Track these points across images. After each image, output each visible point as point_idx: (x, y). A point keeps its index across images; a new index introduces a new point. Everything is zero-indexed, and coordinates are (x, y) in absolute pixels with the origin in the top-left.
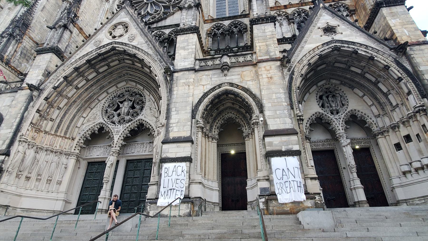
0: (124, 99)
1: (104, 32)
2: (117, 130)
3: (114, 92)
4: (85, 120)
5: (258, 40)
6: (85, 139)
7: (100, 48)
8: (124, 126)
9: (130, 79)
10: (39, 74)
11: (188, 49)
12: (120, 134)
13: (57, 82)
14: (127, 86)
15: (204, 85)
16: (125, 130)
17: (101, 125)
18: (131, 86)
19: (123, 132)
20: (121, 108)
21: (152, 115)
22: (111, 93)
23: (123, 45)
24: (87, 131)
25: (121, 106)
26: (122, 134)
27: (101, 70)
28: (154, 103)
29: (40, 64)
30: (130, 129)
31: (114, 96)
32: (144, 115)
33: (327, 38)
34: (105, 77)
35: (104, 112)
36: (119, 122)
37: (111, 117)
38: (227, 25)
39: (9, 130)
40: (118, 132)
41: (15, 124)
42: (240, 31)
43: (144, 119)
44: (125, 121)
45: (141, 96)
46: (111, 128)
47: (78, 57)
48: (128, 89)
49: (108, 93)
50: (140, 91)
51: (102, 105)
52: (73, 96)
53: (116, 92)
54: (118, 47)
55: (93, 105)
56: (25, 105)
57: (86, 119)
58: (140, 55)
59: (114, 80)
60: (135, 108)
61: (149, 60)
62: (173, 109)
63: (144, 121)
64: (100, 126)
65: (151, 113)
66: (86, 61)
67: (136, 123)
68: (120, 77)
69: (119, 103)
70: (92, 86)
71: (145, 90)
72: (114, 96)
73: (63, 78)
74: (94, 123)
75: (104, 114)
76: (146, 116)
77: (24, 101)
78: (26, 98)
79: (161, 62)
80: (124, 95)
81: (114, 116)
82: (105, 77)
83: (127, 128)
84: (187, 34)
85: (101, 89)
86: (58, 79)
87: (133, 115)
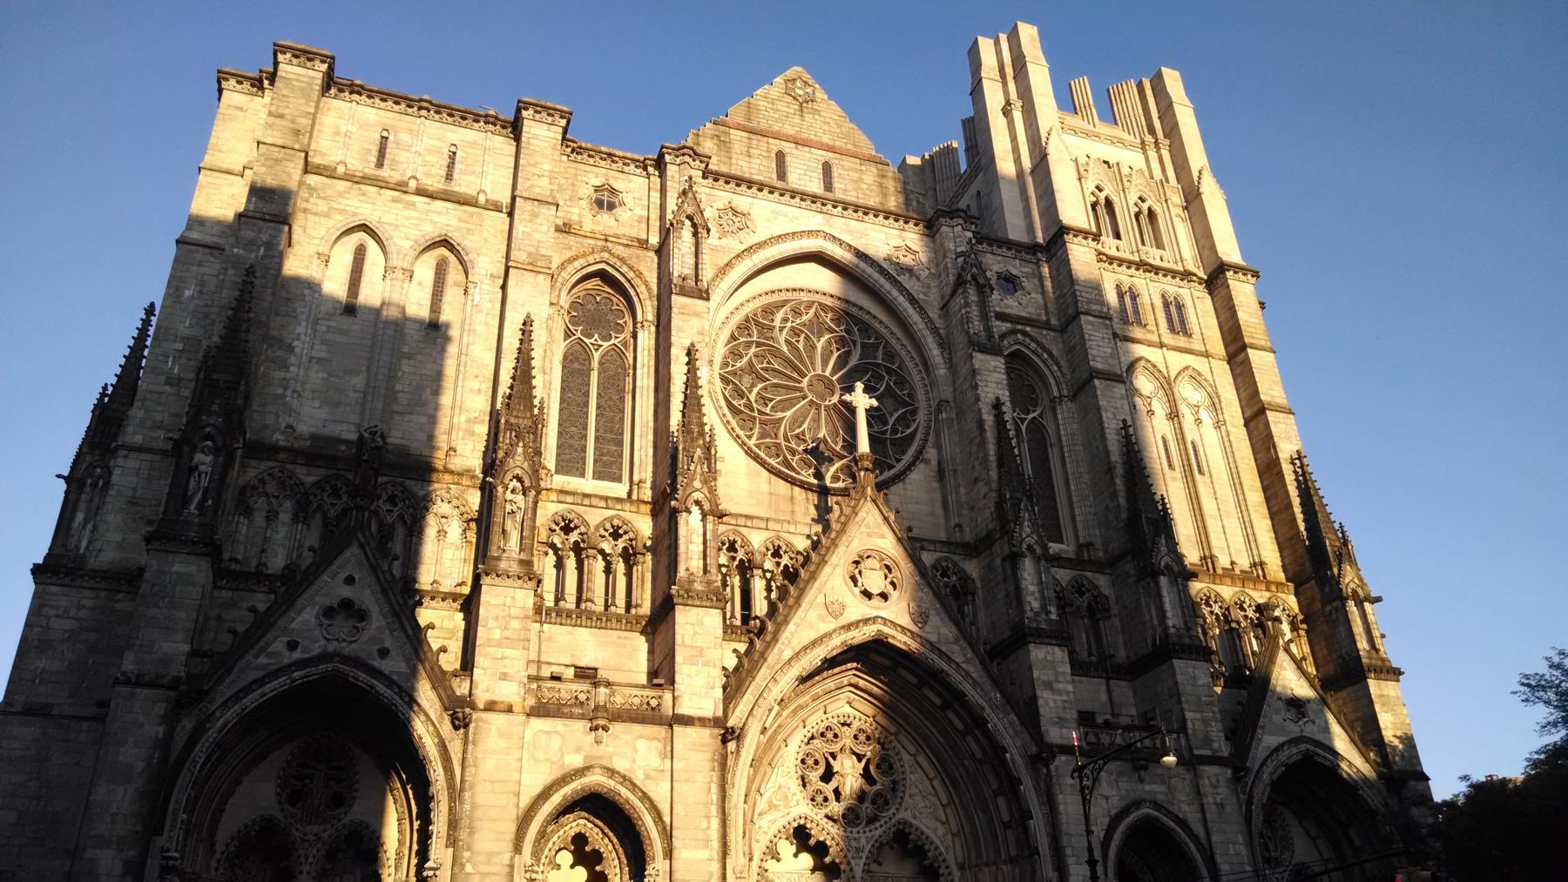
1: (839, 571)
5: (1187, 702)
7: (848, 627)
10: (712, 680)
11: (1060, 693)
13: (768, 716)
15: (1107, 798)
16: (873, 846)
17: (802, 822)
23: (905, 634)
25: (836, 766)
28: (930, 780)
29: (698, 644)
33: (1294, 730)
38: (1064, 584)
39: (704, 854)
41: (714, 835)
42: (1091, 610)
44: (858, 817)
47: (797, 644)
54: (893, 637)
56: (715, 779)
58: (956, 678)
61: (981, 701)
62: (1068, 851)
69: (830, 759)
71: (902, 738)
77: (708, 765)
78: (709, 756)
84: (1047, 644)
87: (873, 802)
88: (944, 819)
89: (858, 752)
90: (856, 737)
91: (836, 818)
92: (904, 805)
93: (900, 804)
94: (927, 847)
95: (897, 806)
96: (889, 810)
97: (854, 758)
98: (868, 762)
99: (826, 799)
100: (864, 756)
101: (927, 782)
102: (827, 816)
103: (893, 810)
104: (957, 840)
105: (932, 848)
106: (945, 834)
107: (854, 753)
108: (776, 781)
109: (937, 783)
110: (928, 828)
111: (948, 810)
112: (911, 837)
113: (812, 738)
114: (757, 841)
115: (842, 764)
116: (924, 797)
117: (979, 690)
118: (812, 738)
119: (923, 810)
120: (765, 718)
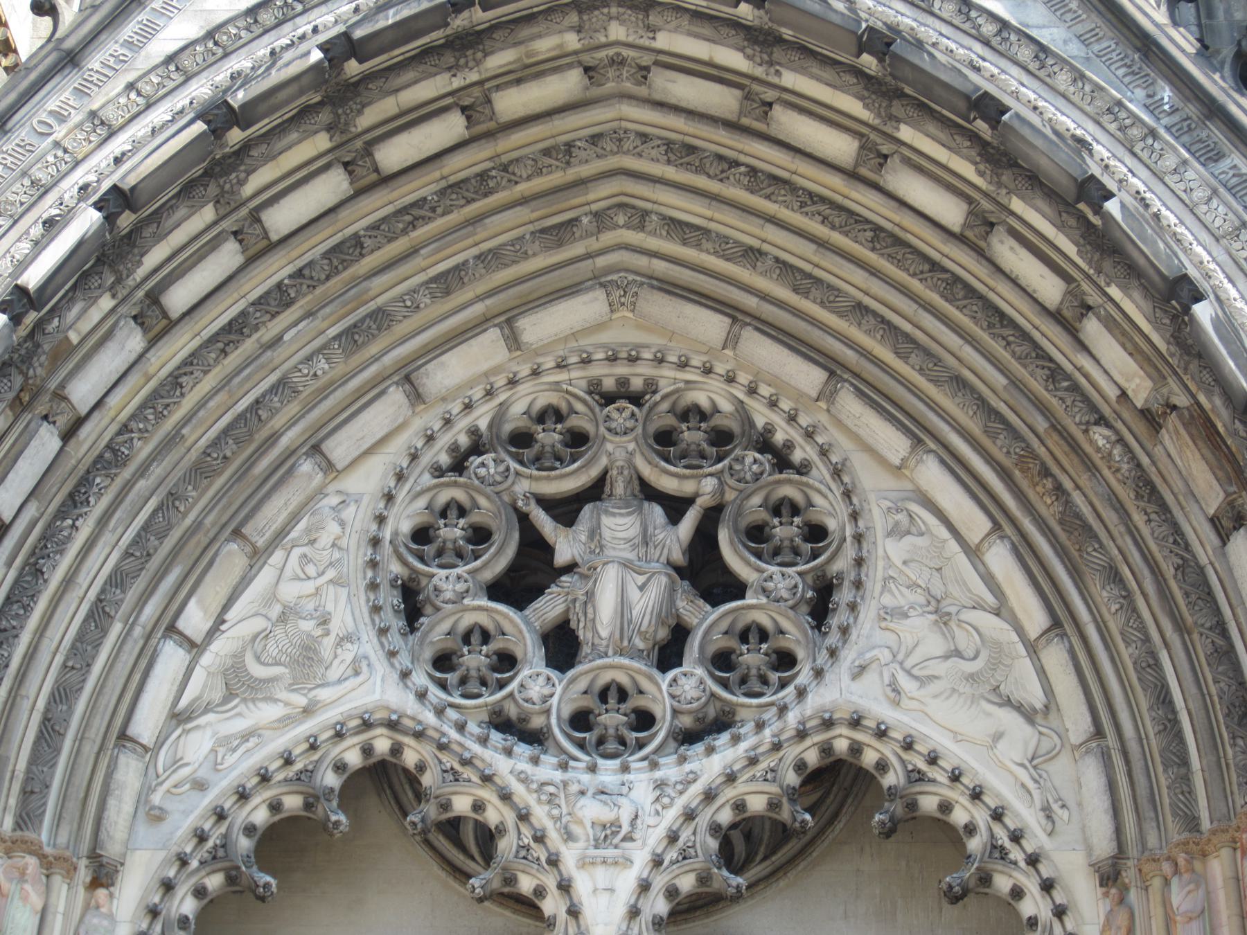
0: (594, 472)
2: (606, 814)
3: (477, 393)
4: (198, 676)
6: (214, 882)
8: (670, 770)
9: (660, 266)
12: (640, 857)
13: (39, 246)
14: (606, 337)
16: (689, 816)
17: (382, 745)
18: (657, 341)
19: (673, 838)
20: (570, 568)
21: (972, 678)
22: (444, 399)
24: (243, 796)
25: (566, 546)
26: (657, 862)
27: (393, 154)
28: (974, 553)
30: (725, 817)
31: (474, 432)
32: (871, 680)
34: (414, 214)
35: (391, 599)
36: (581, 720)
37: (475, 660)
40: (608, 833)
43: (879, 709)
44: (644, 720)
45: (782, 461)
46: (518, 789)
48: (622, 370)
49: (416, 397)
50: (773, 404)
51: (359, 518)
52: (99, 404)
53: (489, 394)
55: (275, 512)
57: (207, 659)
59: (491, 259)
60: (737, 589)
61: (1070, 122)
63: (881, 734)
64: (367, 750)
65: (957, 653)
66: (321, 47)
67: (791, 753)
68: (560, 233)
69: (544, 522)
70: (278, 298)
71: (850, 405)
72: (474, 432)
73: (98, 206)
74: (308, 711)
75: (398, 623)
76: (905, 683)
79: (1211, 156)
80: (578, 440)
81: (506, 661)
82: (414, 214)
83: (709, 796)
85: (352, 338)
86: (47, 208)
87: (722, 661)
88: (1036, 697)
89: (669, 484)
90: (665, 439)
91: (537, 722)
92: (849, 656)
93: (833, 653)
94: (959, 817)
95: (823, 657)
96: (783, 685)
97: (657, 512)
98: (712, 516)
99: (506, 661)
100: (688, 502)
101: (962, 560)
102: (502, 723)
103: (804, 675)
104: (1092, 776)
105: (981, 817)
106: (1035, 762)
107: (649, 493)
108: (271, 597)
109: (1000, 559)
110: (957, 737)
111: (1055, 658)
112: (890, 779)
113: (477, 448)
114: (157, 816)
115: (594, 533)
116: (943, 619)
117: (1063, 80)
118: (477, 448)
119: (939, 668)
120: (25, 247)
